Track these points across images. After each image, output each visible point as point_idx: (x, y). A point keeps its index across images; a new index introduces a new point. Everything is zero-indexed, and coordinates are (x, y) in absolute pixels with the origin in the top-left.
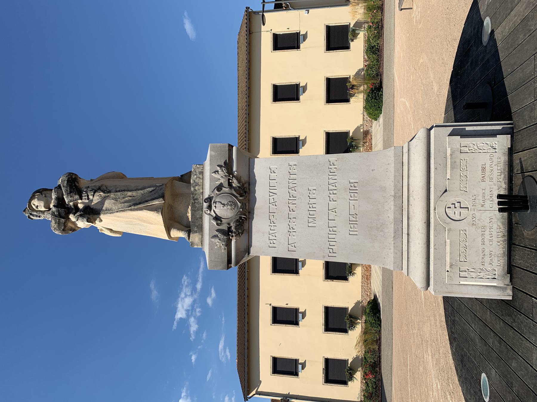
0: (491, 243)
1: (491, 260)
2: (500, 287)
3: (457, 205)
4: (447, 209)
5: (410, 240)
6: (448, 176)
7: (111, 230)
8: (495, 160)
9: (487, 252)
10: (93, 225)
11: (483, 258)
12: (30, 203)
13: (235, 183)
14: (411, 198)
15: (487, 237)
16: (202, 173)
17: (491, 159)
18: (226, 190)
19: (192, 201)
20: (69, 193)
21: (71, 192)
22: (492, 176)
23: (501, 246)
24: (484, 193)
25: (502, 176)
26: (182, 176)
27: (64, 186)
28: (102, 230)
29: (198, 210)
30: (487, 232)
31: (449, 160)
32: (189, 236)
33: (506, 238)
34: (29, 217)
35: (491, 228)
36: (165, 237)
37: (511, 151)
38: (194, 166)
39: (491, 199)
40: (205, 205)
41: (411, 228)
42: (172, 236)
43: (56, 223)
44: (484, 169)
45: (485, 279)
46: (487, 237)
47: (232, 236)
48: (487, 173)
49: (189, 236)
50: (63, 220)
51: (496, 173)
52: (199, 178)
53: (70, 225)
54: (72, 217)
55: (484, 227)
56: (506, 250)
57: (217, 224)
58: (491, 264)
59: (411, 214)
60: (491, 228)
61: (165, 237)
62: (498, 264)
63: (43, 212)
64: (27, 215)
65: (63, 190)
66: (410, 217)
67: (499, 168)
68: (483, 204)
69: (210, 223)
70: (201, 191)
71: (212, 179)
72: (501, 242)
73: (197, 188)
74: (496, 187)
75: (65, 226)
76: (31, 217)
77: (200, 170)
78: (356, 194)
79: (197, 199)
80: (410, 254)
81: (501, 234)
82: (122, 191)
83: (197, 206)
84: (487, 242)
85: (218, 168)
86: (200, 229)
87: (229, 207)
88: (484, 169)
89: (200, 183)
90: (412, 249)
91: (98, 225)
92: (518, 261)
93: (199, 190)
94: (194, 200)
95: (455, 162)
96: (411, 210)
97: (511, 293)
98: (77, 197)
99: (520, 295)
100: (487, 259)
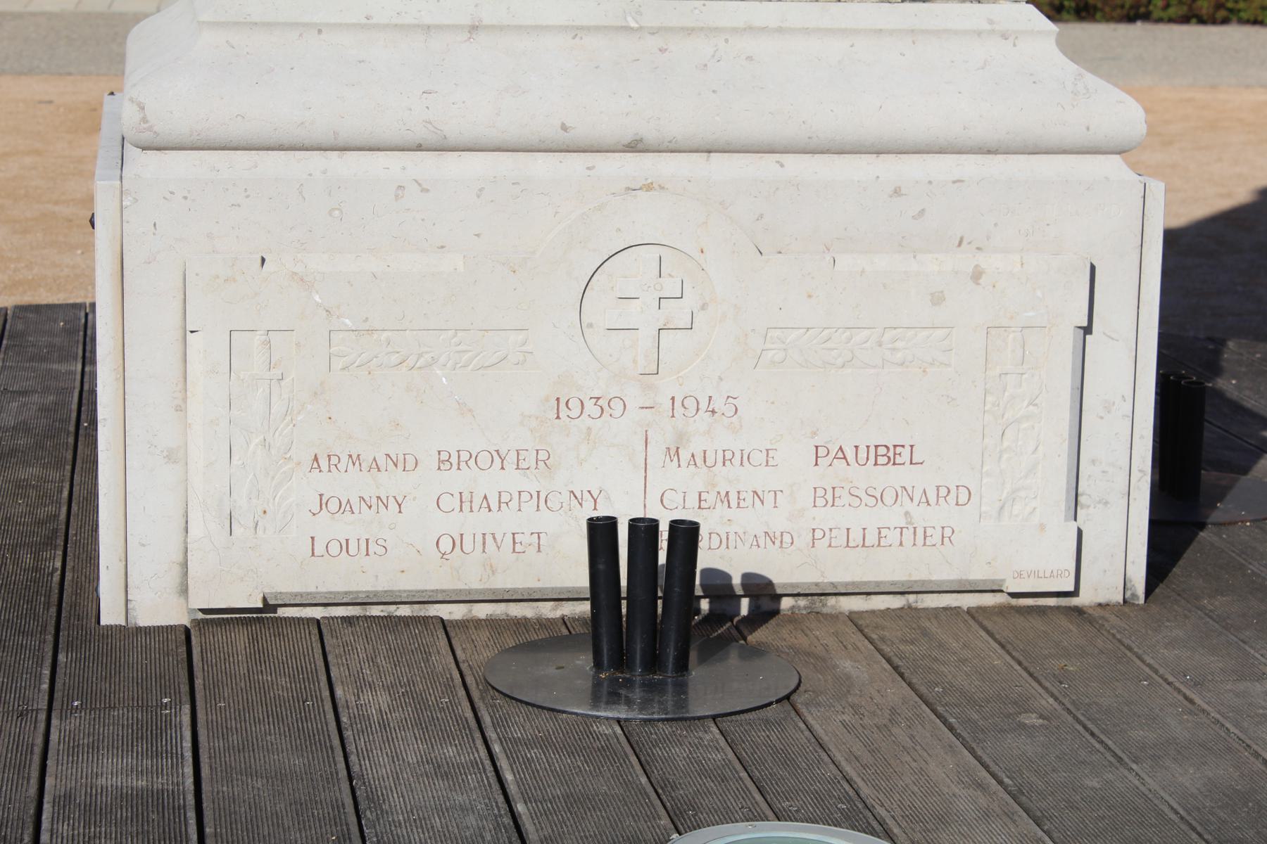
0: (450, 502)
1: (345, 507)
3: (678, 313)
4: (654, 252)
8: (933, 517)
9: (392, 482)
11: (355, 460)
15: (490, 482)
17: (943, 493)
22: (846, 499)
24: (746, 458)
30: (512, 481)
35: (542, 500)
39: (710, 498)
44: (888, 455)
46: (490, 482)
55: (545, 462)
58: (323, 503)
60: (542, 500)
68: (685, 455)
74: (778, 522)
84: (457, 480)
88: (888, 455)
95: (938, 299)
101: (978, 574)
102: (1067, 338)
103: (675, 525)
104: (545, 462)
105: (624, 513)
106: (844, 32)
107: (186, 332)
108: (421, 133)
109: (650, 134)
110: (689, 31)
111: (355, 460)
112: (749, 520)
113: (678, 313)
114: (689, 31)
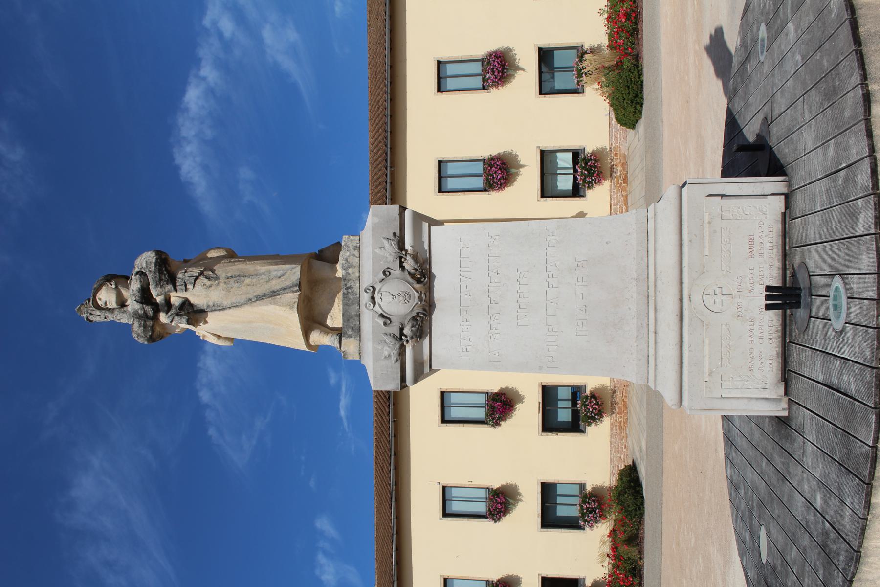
2: (774, 400)
5: (658, 340)
6: (707, 253)
7: (219, 337)
10: (191, 327)
11: (751, 362)
12: (95, 296)
13: (409, 264)
14: (659, 283)
15: (756, 333)
16: (358, 248)
18: (396, 272)
19: (343, 290)
20: (159, 283)
21: (161, 280)
23: (774, 345)
25: (775, 251)
26: (321, 251)
27: (150, 271)
28: (204, 336)
29: (353, 304)
30: (756, 327)
31: (707, 229)
32: (340, 343)
33: (780, 334)
34: (87, 318)
35: (761, 320)
36: (301, 345)
37: (787, 217)
38: (345, 238)
40: (365, 297)
41: (659, 323)
42: (312, 343)
43: (140, 326)
44: (751, 241)
45: (756, 391)
46: (756, 333)
47: (407, 342)
48: (756, 247)
49: (340, 343)
50: (150, 323)
51: (767, 246)
52: (354, 255)
53: (158, 329)
54: (163, 318)
55: (752, 320)
56: (780, 350)
57: (385, 324)
59: (659, 304)
60: (761, 320)
61: (301, 345)
62: (770, 369)
63: (111, 310)
64: (85, 316)
65: (150, 277)
66: (658, 308)
67: (771, 239)
69: (374, 321)
70: (357, 275)
71: (375, 259)
72: (774, 340)
73: (350, 271)
74: (767, 266)
75: (153, 332)
76: (91, 318)
77: (355, 244)
78: (584, 277)
79: (350, 288)
80: (658, 360)
81: (774, 329)
82: (236, 277)
83: (351, 297)
85: (385, 242)
86: (358, 330)
87: (401, 298)
88: (751, 241)
89: (354, 264)
90: (661, 353)
91: (201, 330)
92: (793, 365)
93: (353, 273)
94: (347, 288)
95: (715, 232)
96: (659, 299)
97: (786, 406)
98: (170, 287)
99: (795, 407)
100: (756, 363)
101: (780, 217)
102: (725, 201)
103: (766, 291)
104: (752, 320)
105: (764, 302)
106: (655, 251)
107: (722, 398)
108: (678, 347)
109: (678, 297)
110: (655, 286)
111: (751, 362)
112: (766, 273)
113: (718, 291)
114: (655, 286)
